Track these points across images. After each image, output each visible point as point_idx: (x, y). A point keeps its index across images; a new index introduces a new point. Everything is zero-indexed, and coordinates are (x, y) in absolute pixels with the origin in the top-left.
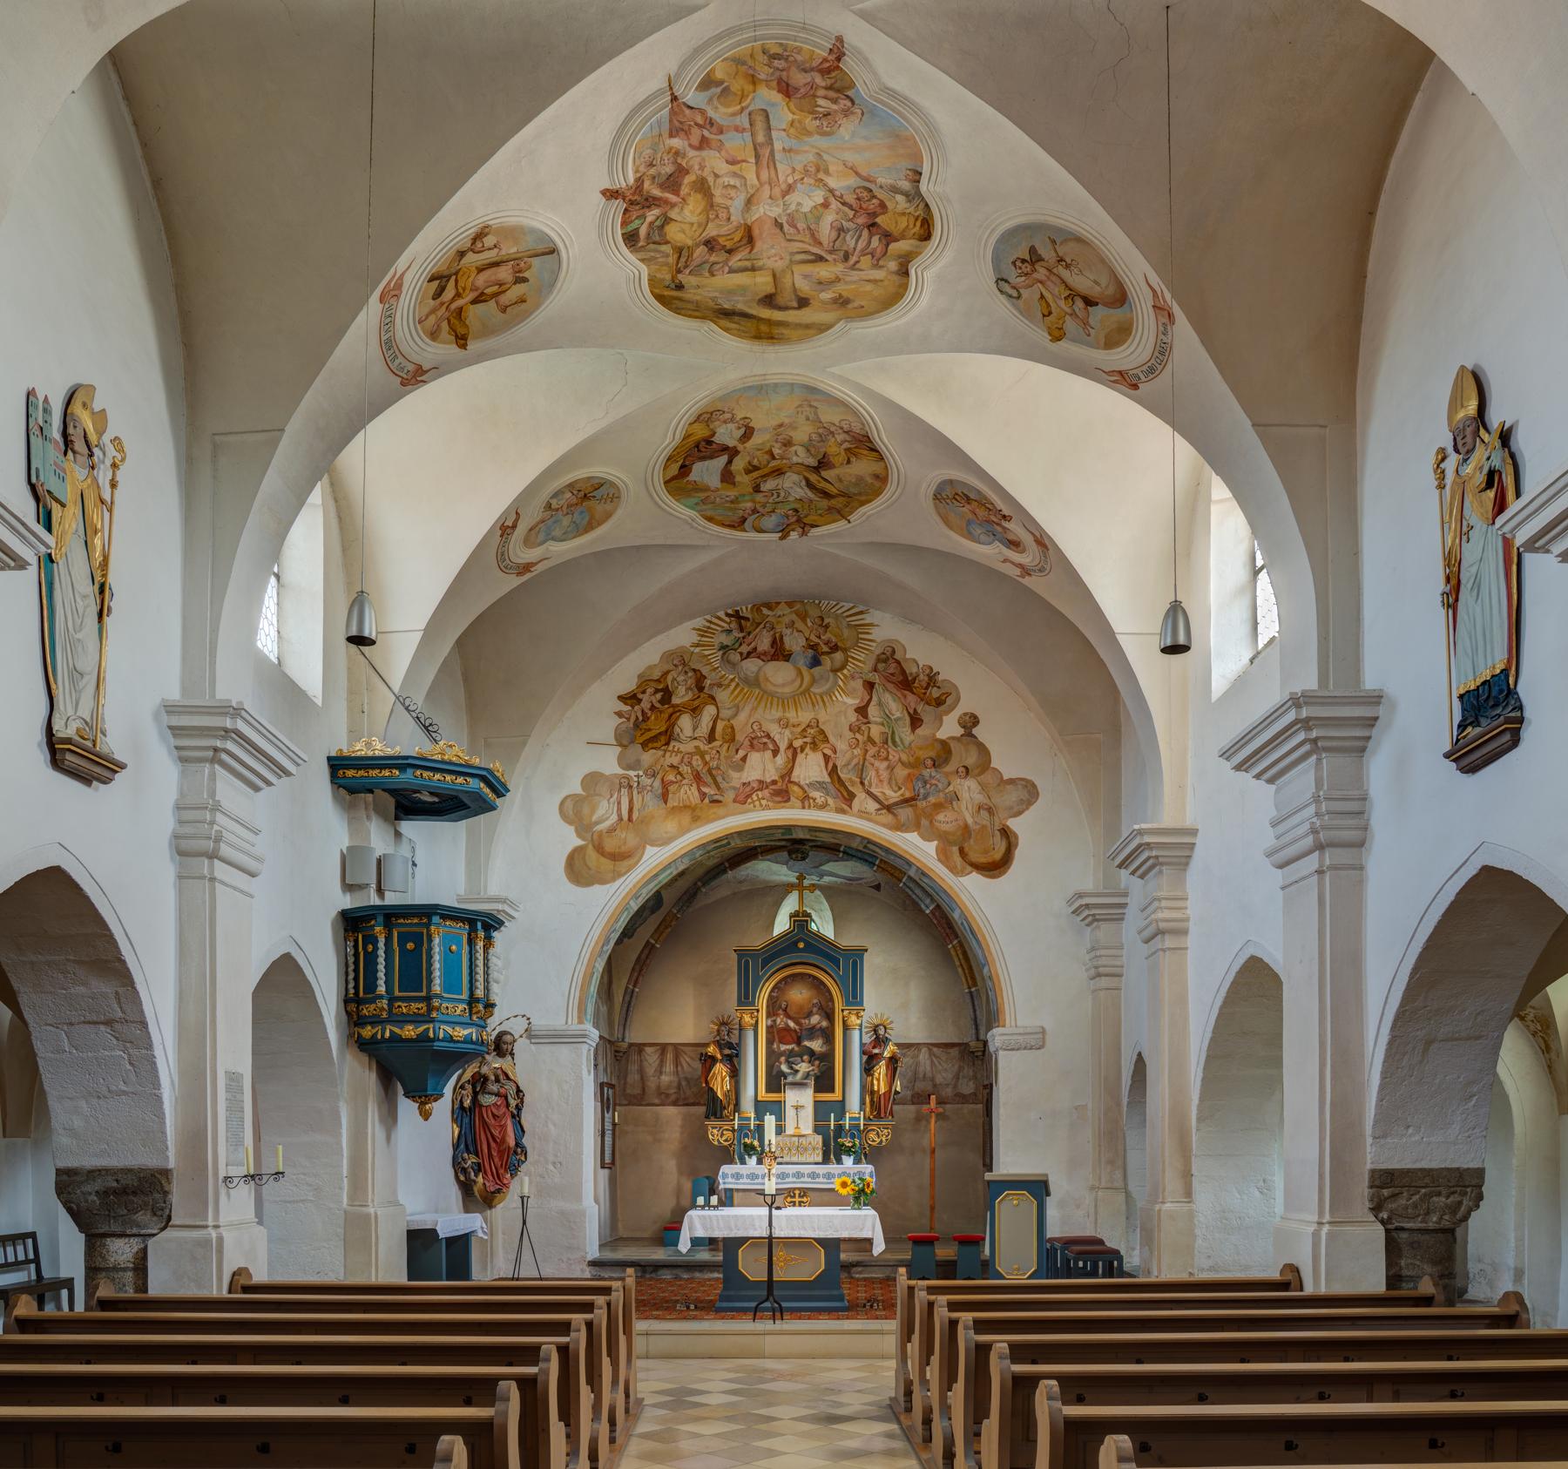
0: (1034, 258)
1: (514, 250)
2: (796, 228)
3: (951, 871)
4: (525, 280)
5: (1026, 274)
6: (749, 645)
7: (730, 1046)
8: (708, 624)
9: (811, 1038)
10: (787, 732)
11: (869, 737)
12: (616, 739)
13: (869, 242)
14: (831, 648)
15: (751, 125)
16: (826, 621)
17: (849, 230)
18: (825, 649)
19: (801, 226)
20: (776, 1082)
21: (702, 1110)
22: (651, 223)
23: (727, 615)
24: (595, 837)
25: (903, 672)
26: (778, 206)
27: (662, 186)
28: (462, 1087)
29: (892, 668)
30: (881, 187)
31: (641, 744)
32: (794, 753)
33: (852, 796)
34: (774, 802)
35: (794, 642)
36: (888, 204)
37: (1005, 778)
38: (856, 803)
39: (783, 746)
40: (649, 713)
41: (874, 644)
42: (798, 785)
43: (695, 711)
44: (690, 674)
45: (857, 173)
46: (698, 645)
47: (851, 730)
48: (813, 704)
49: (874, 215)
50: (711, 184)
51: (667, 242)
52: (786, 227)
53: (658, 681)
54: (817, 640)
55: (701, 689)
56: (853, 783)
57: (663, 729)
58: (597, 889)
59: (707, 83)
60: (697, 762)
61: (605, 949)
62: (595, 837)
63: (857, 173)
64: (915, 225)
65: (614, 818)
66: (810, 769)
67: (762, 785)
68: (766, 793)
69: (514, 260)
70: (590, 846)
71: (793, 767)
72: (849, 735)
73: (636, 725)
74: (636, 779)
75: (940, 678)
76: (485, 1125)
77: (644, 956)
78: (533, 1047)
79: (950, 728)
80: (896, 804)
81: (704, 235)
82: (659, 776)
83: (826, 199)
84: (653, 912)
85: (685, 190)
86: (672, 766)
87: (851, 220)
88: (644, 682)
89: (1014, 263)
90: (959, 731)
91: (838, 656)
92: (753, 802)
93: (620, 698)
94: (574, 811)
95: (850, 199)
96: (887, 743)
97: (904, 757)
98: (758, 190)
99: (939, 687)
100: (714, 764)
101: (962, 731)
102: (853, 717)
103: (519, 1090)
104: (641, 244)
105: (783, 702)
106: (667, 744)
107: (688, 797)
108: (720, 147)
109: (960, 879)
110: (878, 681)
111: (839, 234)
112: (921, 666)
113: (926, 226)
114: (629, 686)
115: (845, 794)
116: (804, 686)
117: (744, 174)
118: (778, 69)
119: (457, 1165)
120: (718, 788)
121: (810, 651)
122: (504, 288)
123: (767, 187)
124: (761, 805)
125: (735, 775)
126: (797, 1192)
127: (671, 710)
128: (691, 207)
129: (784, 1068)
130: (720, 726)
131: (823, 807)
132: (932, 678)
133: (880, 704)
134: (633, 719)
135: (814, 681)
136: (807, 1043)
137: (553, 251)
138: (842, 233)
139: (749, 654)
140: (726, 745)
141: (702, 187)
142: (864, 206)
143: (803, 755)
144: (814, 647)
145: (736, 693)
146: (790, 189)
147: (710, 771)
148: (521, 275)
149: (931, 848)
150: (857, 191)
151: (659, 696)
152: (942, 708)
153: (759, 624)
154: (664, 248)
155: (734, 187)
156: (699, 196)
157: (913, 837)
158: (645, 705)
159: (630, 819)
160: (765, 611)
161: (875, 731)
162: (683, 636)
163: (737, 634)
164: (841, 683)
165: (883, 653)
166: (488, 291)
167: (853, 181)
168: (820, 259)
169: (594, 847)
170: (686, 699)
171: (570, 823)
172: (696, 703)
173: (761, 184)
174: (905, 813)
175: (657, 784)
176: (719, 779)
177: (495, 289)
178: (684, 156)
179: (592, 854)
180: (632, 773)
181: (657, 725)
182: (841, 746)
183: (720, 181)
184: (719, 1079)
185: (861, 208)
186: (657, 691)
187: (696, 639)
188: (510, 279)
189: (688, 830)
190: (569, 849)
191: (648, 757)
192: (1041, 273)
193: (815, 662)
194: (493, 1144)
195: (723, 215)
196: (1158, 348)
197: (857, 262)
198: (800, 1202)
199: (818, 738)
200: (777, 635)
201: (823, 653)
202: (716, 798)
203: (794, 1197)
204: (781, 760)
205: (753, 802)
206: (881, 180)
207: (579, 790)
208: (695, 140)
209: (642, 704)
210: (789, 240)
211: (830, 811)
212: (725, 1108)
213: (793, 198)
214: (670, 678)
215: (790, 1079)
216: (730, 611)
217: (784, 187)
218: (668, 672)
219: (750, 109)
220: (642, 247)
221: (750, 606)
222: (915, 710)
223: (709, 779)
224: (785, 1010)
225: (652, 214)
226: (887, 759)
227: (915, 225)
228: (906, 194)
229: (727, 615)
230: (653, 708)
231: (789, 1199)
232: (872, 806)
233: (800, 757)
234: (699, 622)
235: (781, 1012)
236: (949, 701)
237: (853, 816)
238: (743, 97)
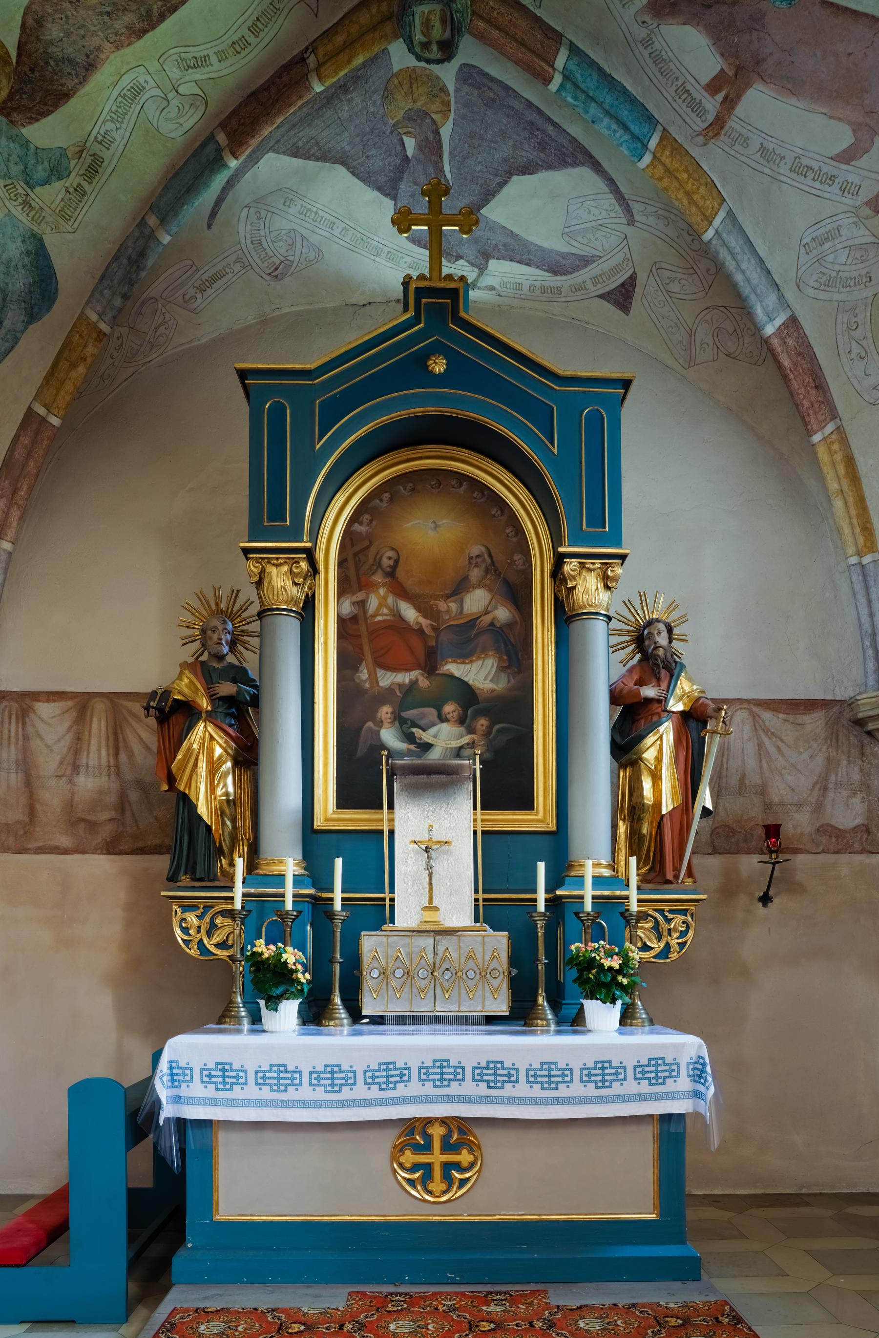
7: (239, 675)
9: (465, 655)
77: (19, 454)
84: (32, 316)
126: (437, 1132)
129: (390, 737)
136: (454, 668)
184: (203, 766)
198: (447, 1167)
203: (427, 1148)
212: (220, 852)
224: (391, 573)
231: (409, 1158)
235: (378, 578)
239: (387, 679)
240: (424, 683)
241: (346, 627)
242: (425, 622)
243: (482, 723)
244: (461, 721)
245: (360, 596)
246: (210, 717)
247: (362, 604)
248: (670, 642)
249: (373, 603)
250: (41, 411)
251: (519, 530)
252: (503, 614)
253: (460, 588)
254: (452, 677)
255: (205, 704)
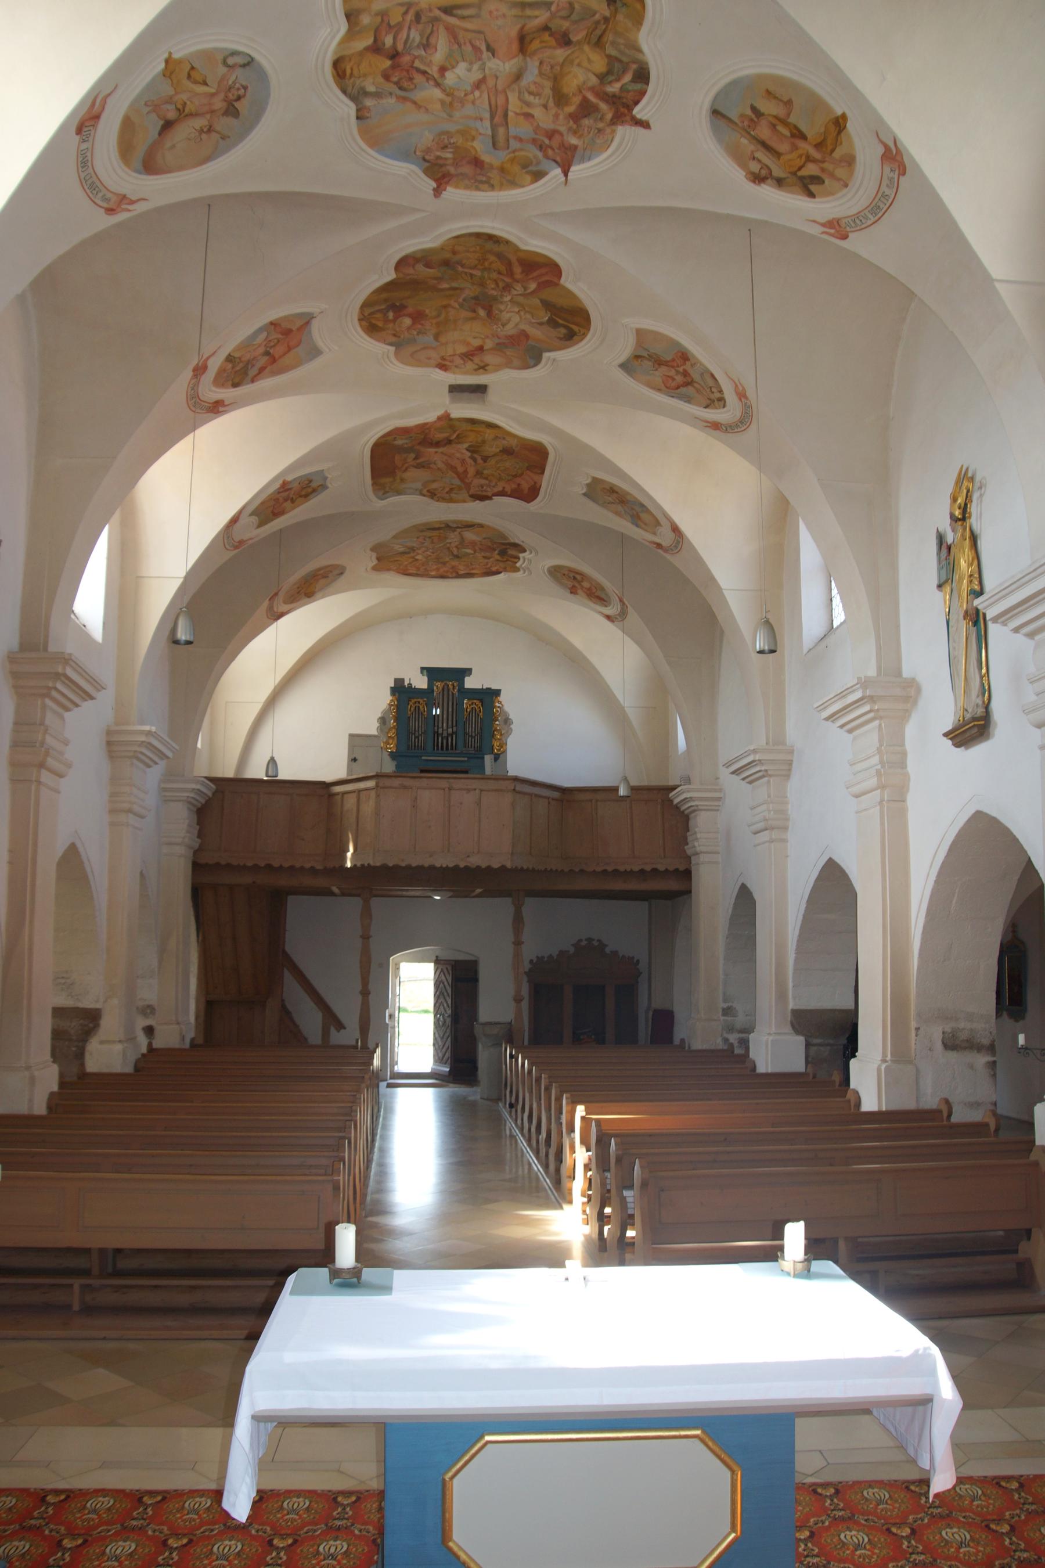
0: (231, 111)
1: (744, 141)
2: (473, 46)
4: (754, 109)
5: (230, 88)
13: (395, 39)
15: (508, 140)
17: (418, 47)
19: (468, 48)
22: (618, 80)
26: (490, 69)
27: (596, 109)
30: (391, 94)
36: (381, 80)
45: (415, 103)
49: (393, 67)
50: (551, 99)
51: (609, 57)
52: (484, 48)
59: (538, 175)
63: (415, 103)
64: (352, 69)
69: (749, 133)
81: (569, 52)
83: (443, 76)
85: (577, 100)
87: (416, 57)
89: (245, 88)
95: (419, 78)
98: (509, 86)
104: (635, 66)
108: (537, 129)
111: (428, 39)
113: (340, 73)
117: (519, 103)
118: (483, 175)
122: (774, 121)
123: (500, 88)
128: (575, 82)
137: (715, 113)
138: (425, 42)
141: (560, 98)
142: (405, 73)
146: (478, 85)
148: (753, 116)
150: (412, 87)
154: (613, 52)
155: (531, 93)
156: (565, 90)
166: (786, 132)
167: (419, 95)
168: (447, 10)
173: (504, 91)
177: (780, 128)
178: (570, 129)
183: (543, 101)
185: (408, 71)
188: (764, 123)
192: (219, 104)
195: (546, 68)
196: (99, 184)
197: (406, 13)
206: (392, 101)
208: (557, 139)
210: (480, 32)
213: (476, 75)
217: (483, 87)
219: (507, 151)
220: (634, 62)
225: (614, 88)
227: (352, 69)
228: (367, 94)
238: (512, 160)
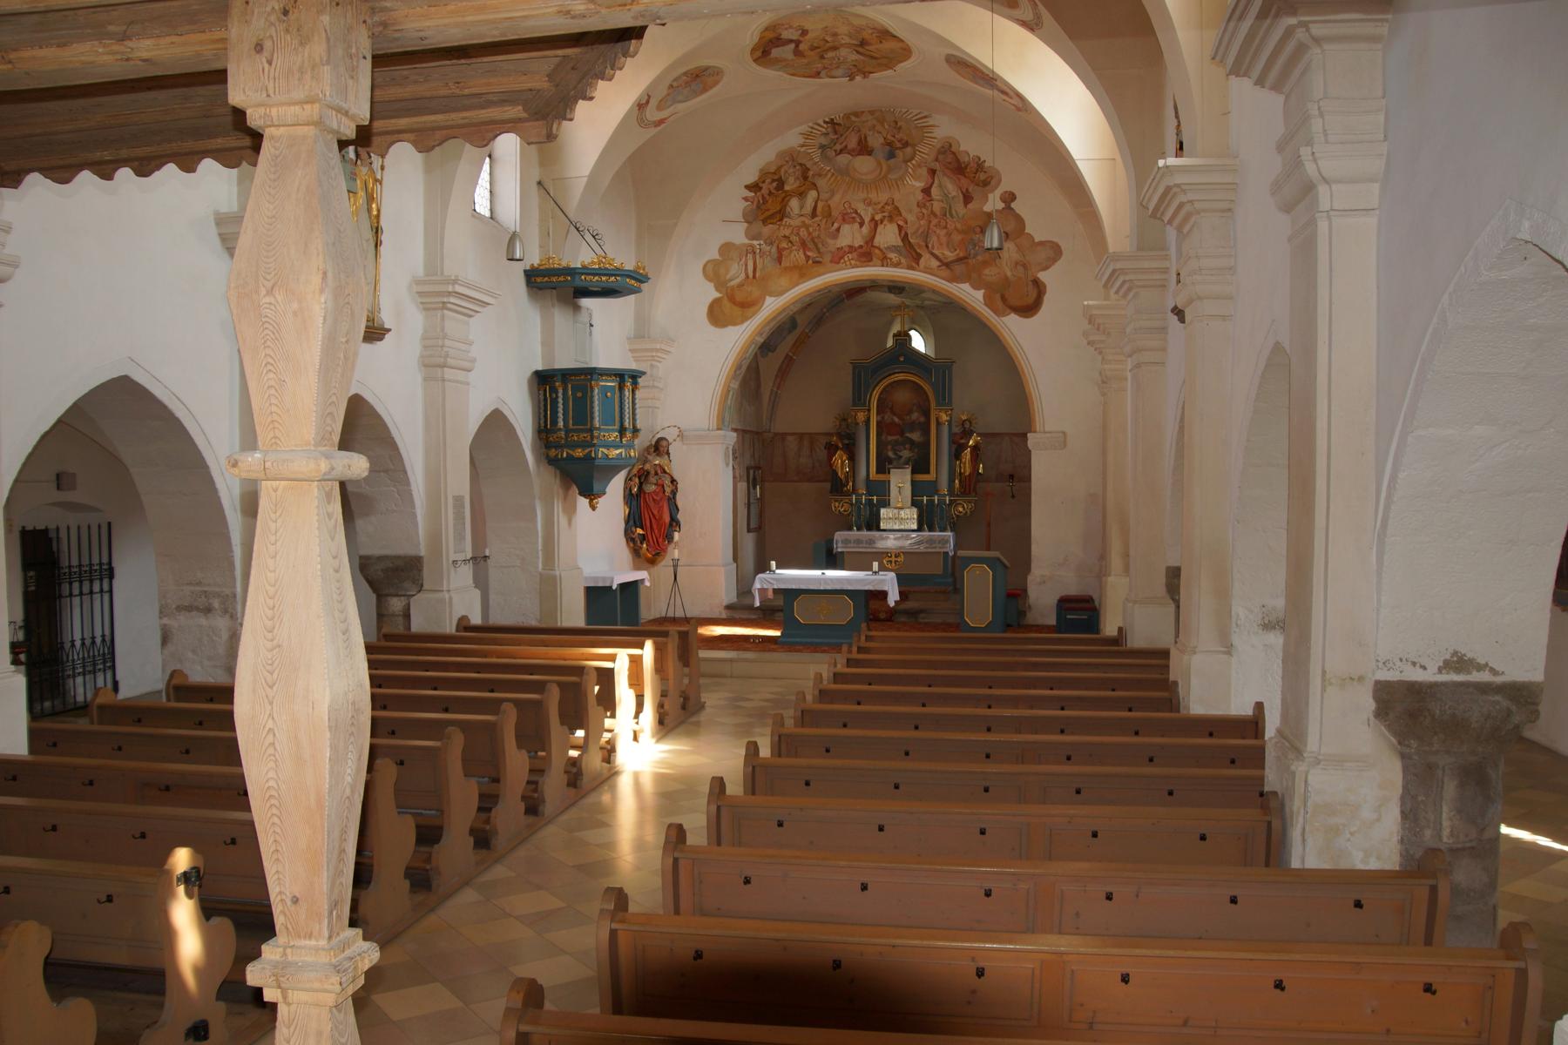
3: (995, 313)
6: (841, 144)
8: (810, 130)
10: (870, 210)
11: (932, 211)
12: (744, 218)
14: (903, 144)
16: (899, 124)
18: (899, 145)
20: (883, 467)
21: (828, 485)
23: (825, 122)
24: (729, 291)
25: (958, 160)
28: (630, 479)
29: (950, 158)
31: (763, 220)
32: (875, 224)
33: (919, 256)
34: (860, 261)
35: (875, 141)
37: (1036, 241)
38: (922, 261)
39: (867, 220)
40: (768, 197)
41: (935, 140)
42: (879, 248)
43: (801, 195)
44: (798, 167)
46: (802, 146)
47: (918, 206)
48: (890, 188)
53: (774, 173)
54: (893, 139)
55: (805, 178)
56: (920, 246)
57: (778, 209)
58: (730, 329)
60: (803, 233)
61: (738, 372)
62: (729, 291)
65: (743, 276)
66: (888, 236)
67: (851, 249)
68: (855, 254)
70: (725, 297)
71: (875, 234)
72: (917, 210)
73: (758, 207)
74: (758, 247)
75: (987, 164)
76: (648, 506)
78: (685, 447)
79: (993, 203)
80: (952, 262)
82: (775, 245)
86: (785, 236)
88: (764, 174)
90: (1001, 206)
91: (909, 150)
92: (845, 262)
93: (747, 187)
94: (713, 272)
96: (945, 215)
97: (959, 226)
99: (985, 172)
100: (816, 234)
101: (1003, 205)
102: (920, 196)
103: (673, 481)
105: (867, 186)
106: (781, 220)
107: (797, 260)
109: (1003, 319)
110: (938, 168)
112: (971, 156)
114: (751, 179)
115: (914, 254)
116: (883, 174)
119: (628, 534)
120: (819, 252)
121: (888, 147)
124: (851, 264)
125: (831, 241)
127: (784, 195)
130: (820, 205)
131: (897, 265)
132: (980, 166)
133: (940, 186)
134: (755, 203)
135: (890, 170)
139: (841, 151)
140: (824, 221)
143: (883, 226)
144: (890, 144)
145: (832, 179)
147: (813, 240)
149: (979, 295)
151: (775, 184)
152: (987, 188)
153: (849, 128)
157: (966, 287)
158: (765, 191)
159: (754, 277)
160: (853, 118)
161: (937, 207)
162: (792, 139)
163: (832, 136)
164: (910, 170)
165: (943, 147)
169: (728, 297)
170: (795, 186)
171: (710, 281)
172: (803, 189)
174: (959, 268)
175: (774, 250)
176: (820, 246)
179: (727, 304)
180: (755, 243)
181: (773, 207)
182: (911, 218)
186: (773, 181)
187: (801, 141)
189: (797, 285)
190: (710, 299)
191: (767, 230)
193: (891, 155)
194: (653, 520)
199: (894, 214)
200: (863, 136)
201: (897, 148)
202: (817, 259)
204: (865, 229)
205: (845, 262)
207: (717, 256)
209: (763, 191)
211: (902, 268)
214: (783, 170)
215: (895, 463)
216: (827, 120)
218: (782, 166)
221: (841, 115)
222: (967, 190)
223: (811, 245)
226: (946, 227)
229: (825, 122)
230: (770, 193)
232: (935, 263)
233: (880, 228)
234: (804, 128)
236: (993, 183)
237: (920, 271)
239: (890, 438)
240: (900, 439)
241: (878, 423)
242: (901, 422)
243: (916, 450)
244: (910, 449)
245: (882, 415)
246: (841, 449)
247: (883, 418)
248: (971, 426)
249: (886, 417)
250: (791, 354)
251: (927, 396)
252: (922, 419)
253: (910, 412)
254: (907, 437)
255: (840, 445)
